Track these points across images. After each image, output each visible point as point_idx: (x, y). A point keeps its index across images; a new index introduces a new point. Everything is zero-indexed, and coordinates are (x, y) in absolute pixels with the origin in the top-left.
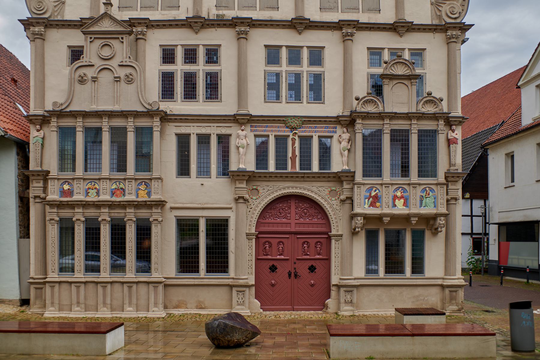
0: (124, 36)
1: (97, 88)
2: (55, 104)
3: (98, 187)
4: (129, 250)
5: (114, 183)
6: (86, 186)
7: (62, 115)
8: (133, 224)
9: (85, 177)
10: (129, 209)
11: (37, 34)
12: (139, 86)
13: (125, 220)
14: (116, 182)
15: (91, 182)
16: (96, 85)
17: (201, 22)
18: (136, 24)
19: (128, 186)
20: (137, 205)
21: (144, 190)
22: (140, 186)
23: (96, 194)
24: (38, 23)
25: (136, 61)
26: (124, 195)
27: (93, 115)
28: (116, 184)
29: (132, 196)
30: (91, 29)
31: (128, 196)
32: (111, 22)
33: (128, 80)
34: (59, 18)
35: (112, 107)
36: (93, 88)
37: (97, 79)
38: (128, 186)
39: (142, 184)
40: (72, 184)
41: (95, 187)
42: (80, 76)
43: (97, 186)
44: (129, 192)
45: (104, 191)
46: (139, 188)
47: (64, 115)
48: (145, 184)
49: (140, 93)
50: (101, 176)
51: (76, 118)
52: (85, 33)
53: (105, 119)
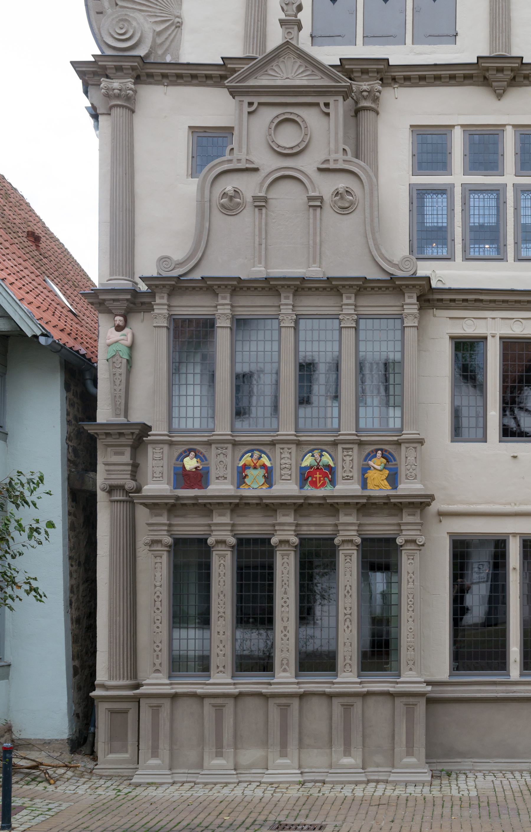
0: (331, 100)
1: (266, 225)
2: (164, 259)
3: (268, 464)
4: (345, 614)
5: (308, 453)
6: (240, 460)
7: (180, 288)
8: (355, 552)
9: (237, 439)
10: (346, 515)
11: (118, 97)
12: (368, 220)
13: (336, 541)
14: (312, 451)
15: (251, 451)
16: (264, 216)
17: (512, 69)
18: (356, 74)
19: (344, 460)
20: (364, 505)
21: (380, 471)
22: (370, 460)
23: (263, 480)
24: (119, 69)
25: (357, 156)
26: (333, 483)
27: (256, 288)
28: (313, 456)
29: (352, 484)
30: (251, 82)
31: (343, 484)
32: (300, 66)
33: (343, 205)
34: (168, 59)
35: (305, 271)
36: (257, 223)
37: (266, 202)
38: (344, 460)
39: (375, 456)
40: (204, 456)
41: (260, 462)
42: (224, 195)
43: (265, 460)
44: (345, 475)
45: (283, 472)
46: (368, 465)
47: (187, 288)
48: (382, 454)
49: (370, 236)
50: (277, 436)
51: (217, 295)
52: (234, 93)
53: (287, 298)
